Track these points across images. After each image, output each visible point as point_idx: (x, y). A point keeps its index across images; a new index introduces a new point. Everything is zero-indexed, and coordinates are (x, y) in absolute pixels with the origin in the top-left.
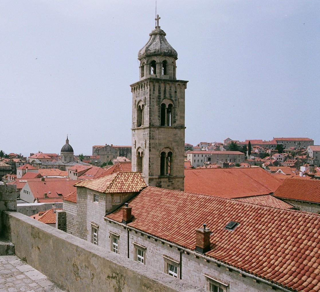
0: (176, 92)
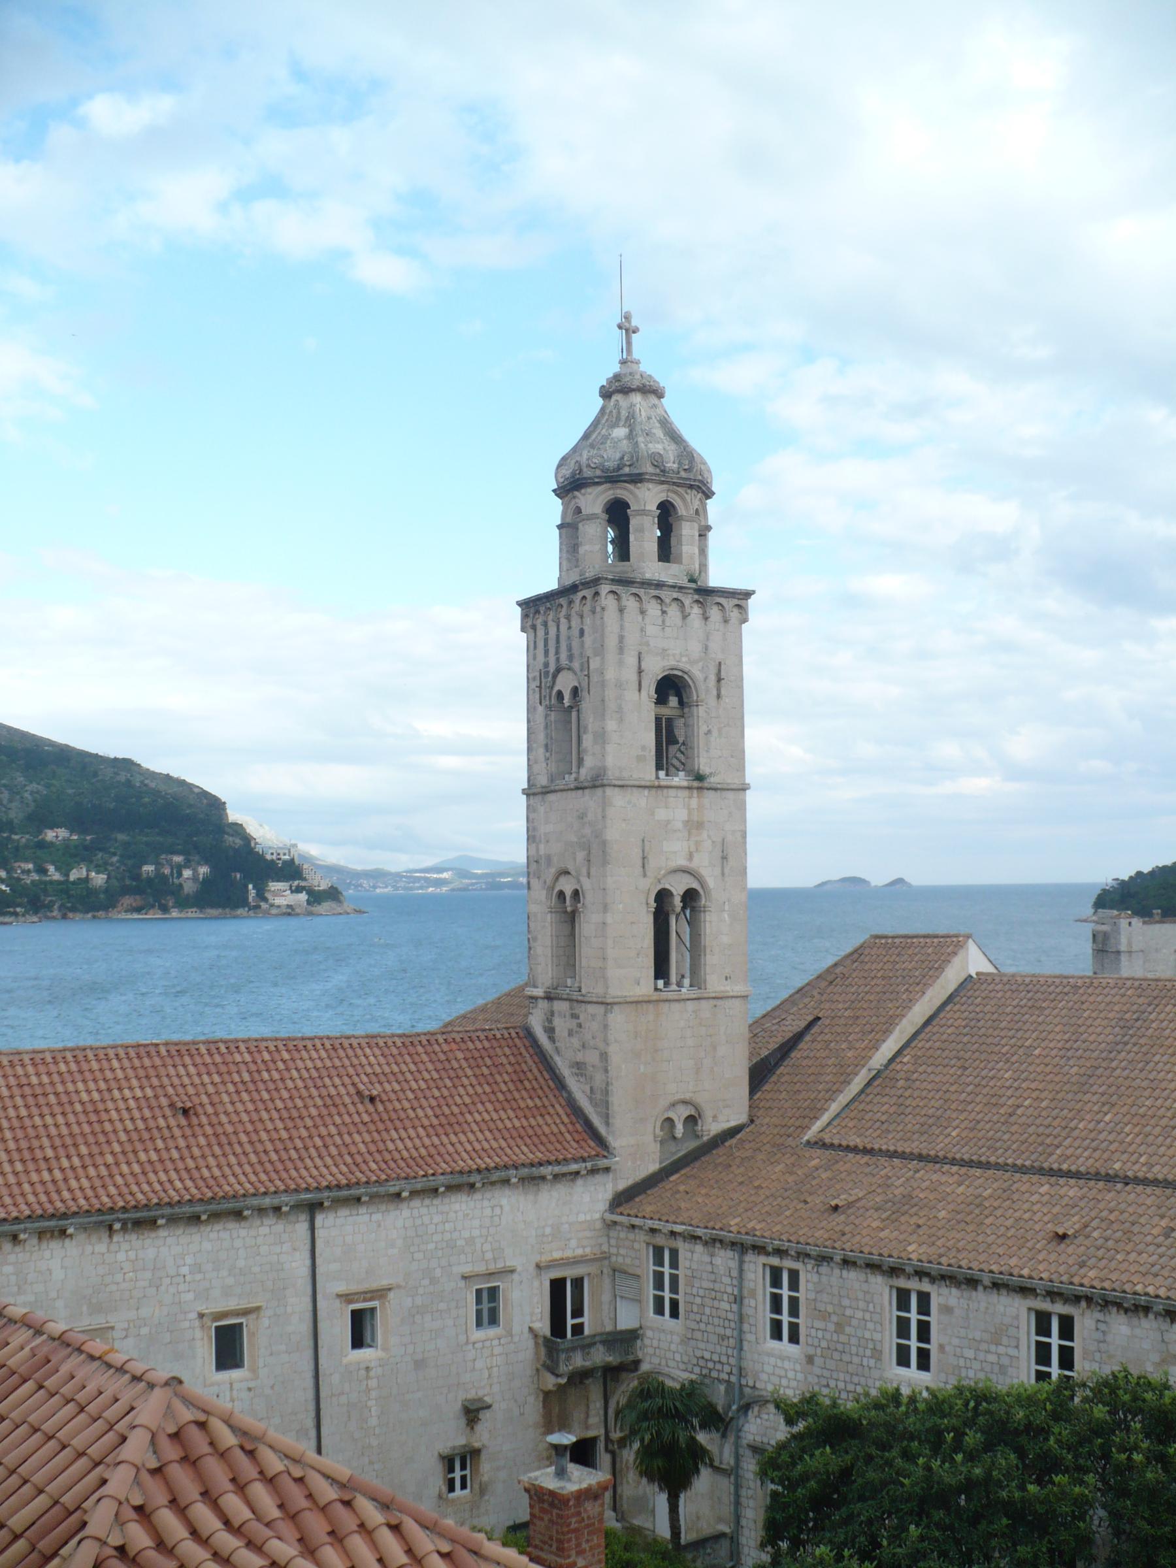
0: (582, 632)
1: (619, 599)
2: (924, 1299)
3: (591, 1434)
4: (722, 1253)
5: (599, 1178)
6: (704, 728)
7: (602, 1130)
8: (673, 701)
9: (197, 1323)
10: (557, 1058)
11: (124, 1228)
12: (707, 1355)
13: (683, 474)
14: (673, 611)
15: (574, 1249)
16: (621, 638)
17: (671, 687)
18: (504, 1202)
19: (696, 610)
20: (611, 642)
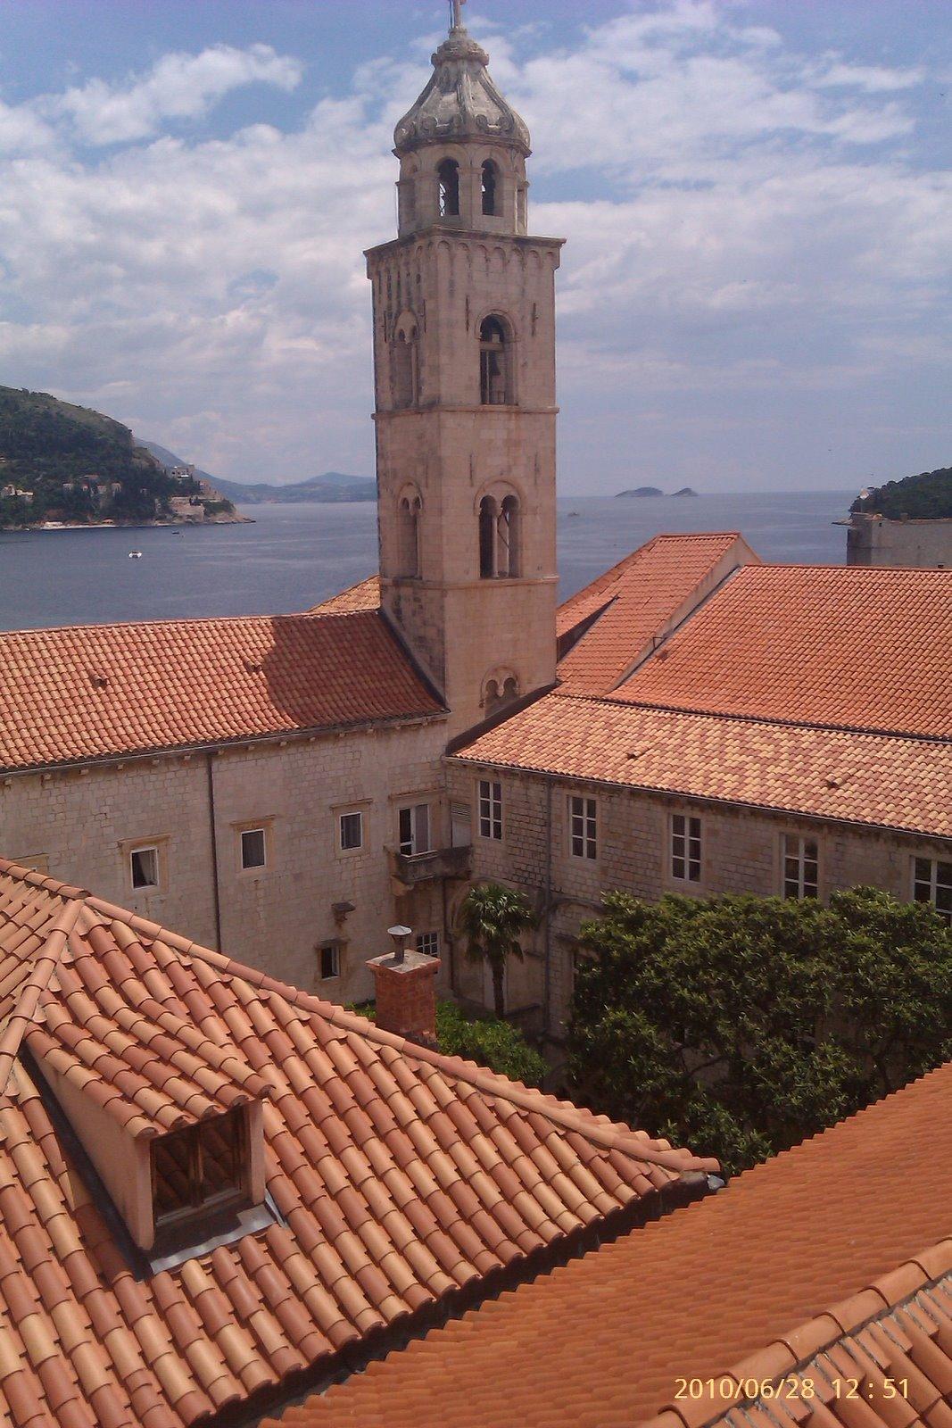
0: (419, 278)
1: (449, 248)
2: (695, 825)
3: (433, 929)
4: (535, 786)
5: (437, 728)
6: (521, 361)
7: (440, 690)
8: (496, 338)
9: (117, 851)
10: (404, 634)
11: (54, 779)
12: (523, 867)
13: (505, 135)
14: (496, 260)
15: (419, 784)
16: (452, 284)
17: (493, 326)
18: (362, 748)
19: (515, 258)
20: (444, 286)
